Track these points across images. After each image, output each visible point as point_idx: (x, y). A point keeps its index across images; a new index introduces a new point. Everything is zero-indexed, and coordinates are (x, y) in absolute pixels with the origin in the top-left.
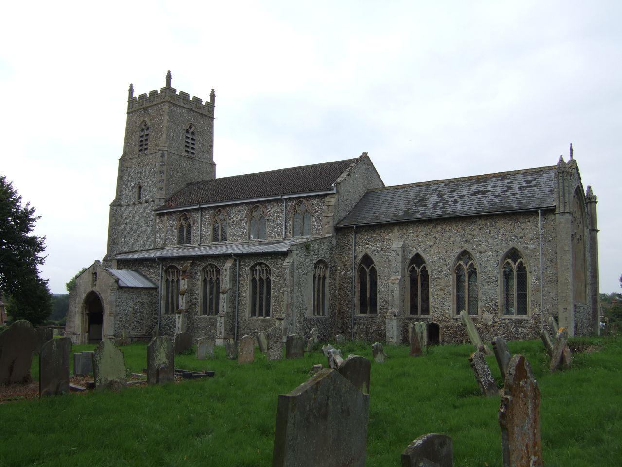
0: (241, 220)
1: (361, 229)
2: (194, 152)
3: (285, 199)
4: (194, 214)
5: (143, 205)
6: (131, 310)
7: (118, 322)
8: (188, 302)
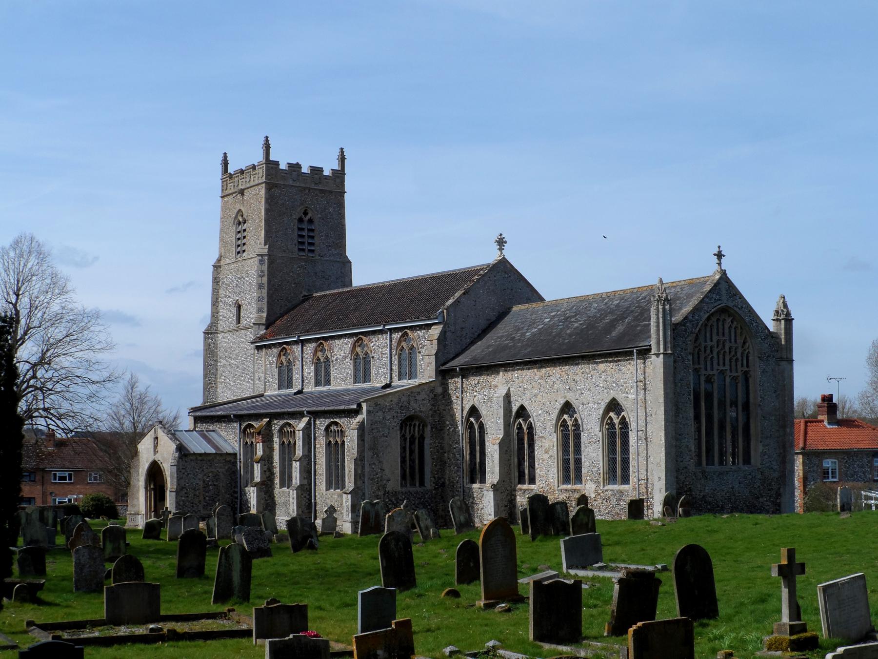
0: (345, 358)
1: (468, 372)
2: (312, 248)
3: (390, 329)
4: (294, 347)
5: (242, 332)
6: (201, 483)
7: (183, 498)
8: (265, 471)
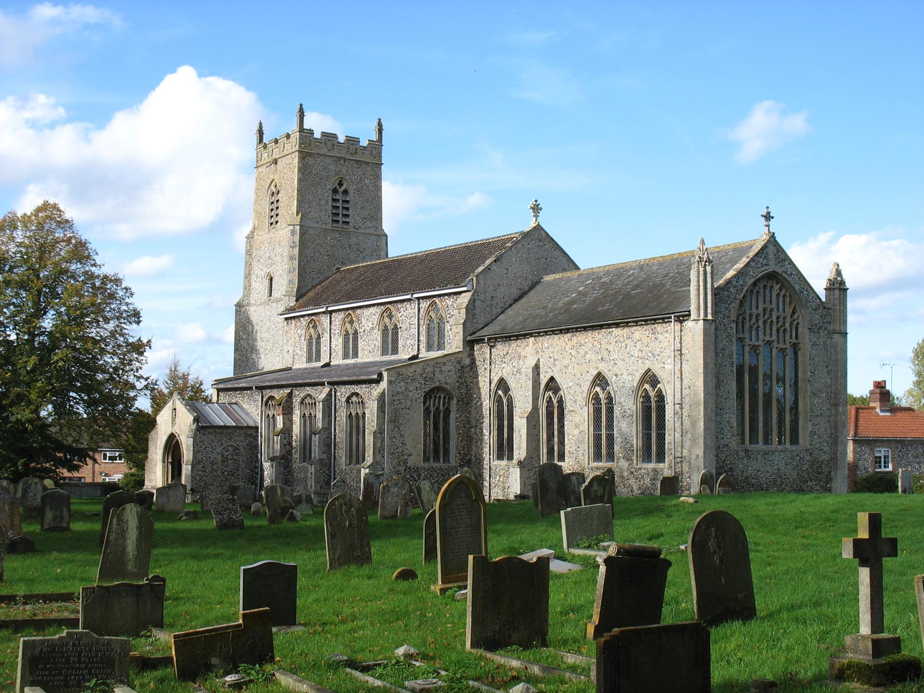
2: (347, 220)
3: (418, 299)
5: (274, 304)
6: (220, 457)
7: (200, 473)
8: (285, 445)
